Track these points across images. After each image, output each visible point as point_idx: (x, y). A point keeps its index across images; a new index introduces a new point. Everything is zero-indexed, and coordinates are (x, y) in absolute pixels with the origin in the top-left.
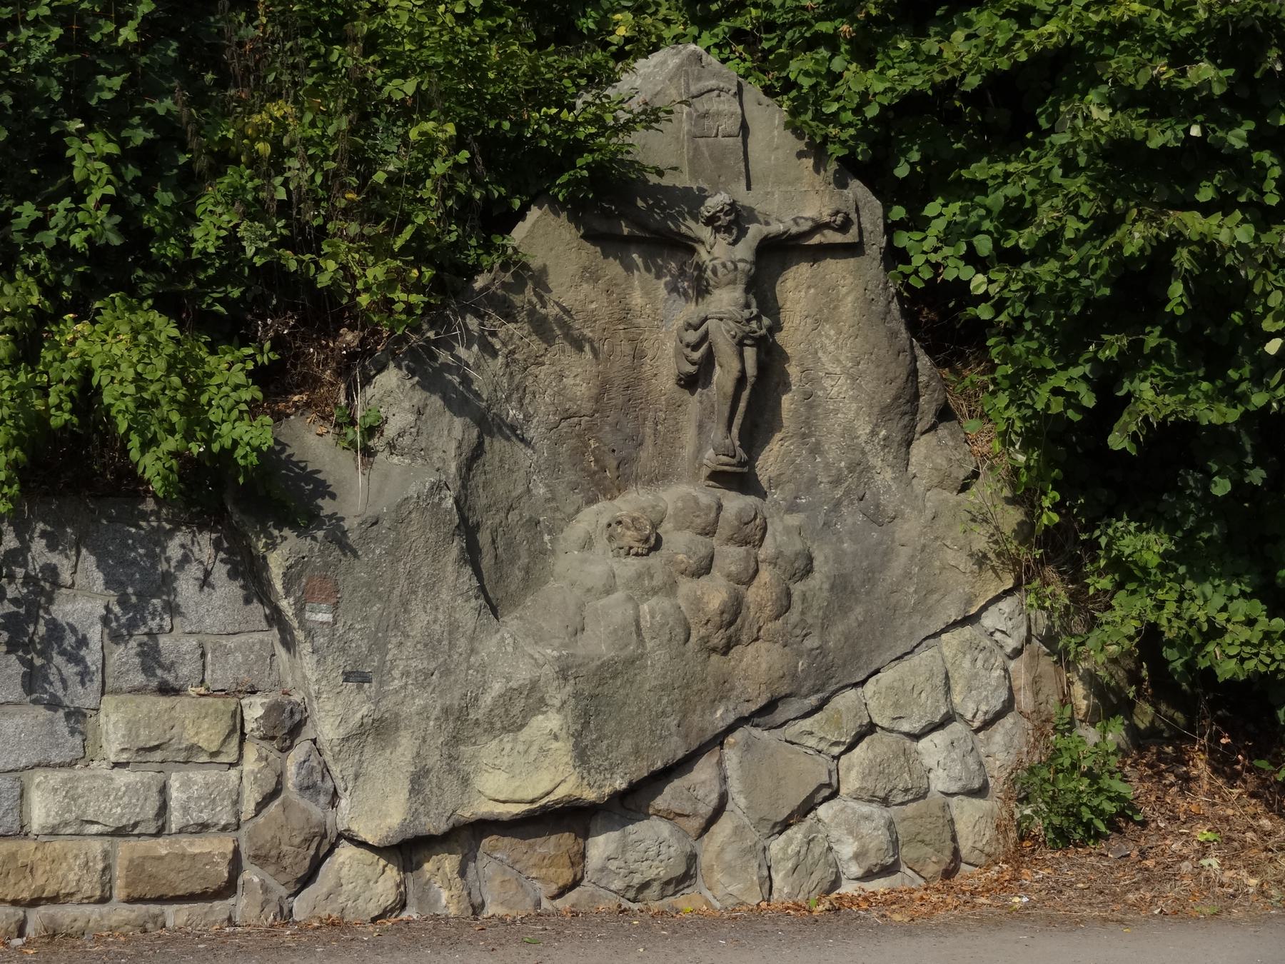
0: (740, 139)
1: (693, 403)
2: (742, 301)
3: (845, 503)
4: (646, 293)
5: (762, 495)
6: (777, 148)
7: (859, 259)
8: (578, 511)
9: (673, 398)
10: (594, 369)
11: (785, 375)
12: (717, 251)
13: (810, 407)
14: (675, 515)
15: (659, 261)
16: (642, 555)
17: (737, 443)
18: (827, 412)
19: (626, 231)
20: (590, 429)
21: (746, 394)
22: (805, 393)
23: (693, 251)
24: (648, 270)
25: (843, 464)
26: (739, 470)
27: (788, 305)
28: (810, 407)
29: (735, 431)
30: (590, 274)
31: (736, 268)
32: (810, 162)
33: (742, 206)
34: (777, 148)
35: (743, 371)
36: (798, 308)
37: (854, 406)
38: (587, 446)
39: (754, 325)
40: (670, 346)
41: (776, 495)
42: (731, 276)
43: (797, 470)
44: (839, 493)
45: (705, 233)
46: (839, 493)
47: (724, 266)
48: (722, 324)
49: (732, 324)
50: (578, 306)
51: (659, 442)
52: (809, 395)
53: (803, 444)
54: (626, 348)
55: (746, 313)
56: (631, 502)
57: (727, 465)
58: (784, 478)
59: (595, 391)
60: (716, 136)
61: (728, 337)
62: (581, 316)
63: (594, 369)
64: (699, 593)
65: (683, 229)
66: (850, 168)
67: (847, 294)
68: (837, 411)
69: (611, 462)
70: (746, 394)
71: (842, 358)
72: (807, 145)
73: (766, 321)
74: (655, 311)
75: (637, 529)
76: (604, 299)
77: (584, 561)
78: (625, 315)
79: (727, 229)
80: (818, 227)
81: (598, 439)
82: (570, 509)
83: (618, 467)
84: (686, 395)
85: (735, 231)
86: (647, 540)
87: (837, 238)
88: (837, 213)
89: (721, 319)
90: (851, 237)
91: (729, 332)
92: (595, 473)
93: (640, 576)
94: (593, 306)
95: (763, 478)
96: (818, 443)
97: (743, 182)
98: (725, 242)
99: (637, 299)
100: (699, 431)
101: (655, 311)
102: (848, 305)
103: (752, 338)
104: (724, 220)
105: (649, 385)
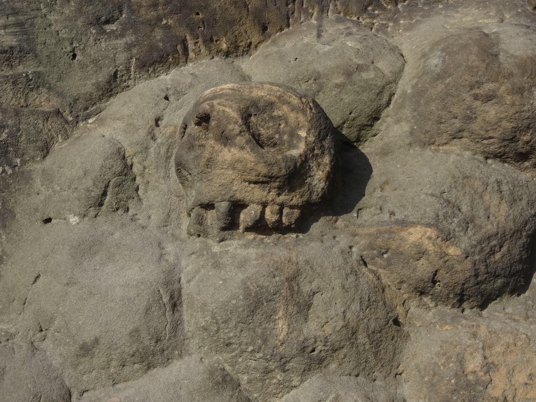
8: (112, 87)
14: (419, 93)
16: (280, 228)
56: (294, 62)
64: (474, 364)
75: (258, 141)
77: (86, 249)
82: (82, 82)
86: (294, 176)
93: (257, 304)
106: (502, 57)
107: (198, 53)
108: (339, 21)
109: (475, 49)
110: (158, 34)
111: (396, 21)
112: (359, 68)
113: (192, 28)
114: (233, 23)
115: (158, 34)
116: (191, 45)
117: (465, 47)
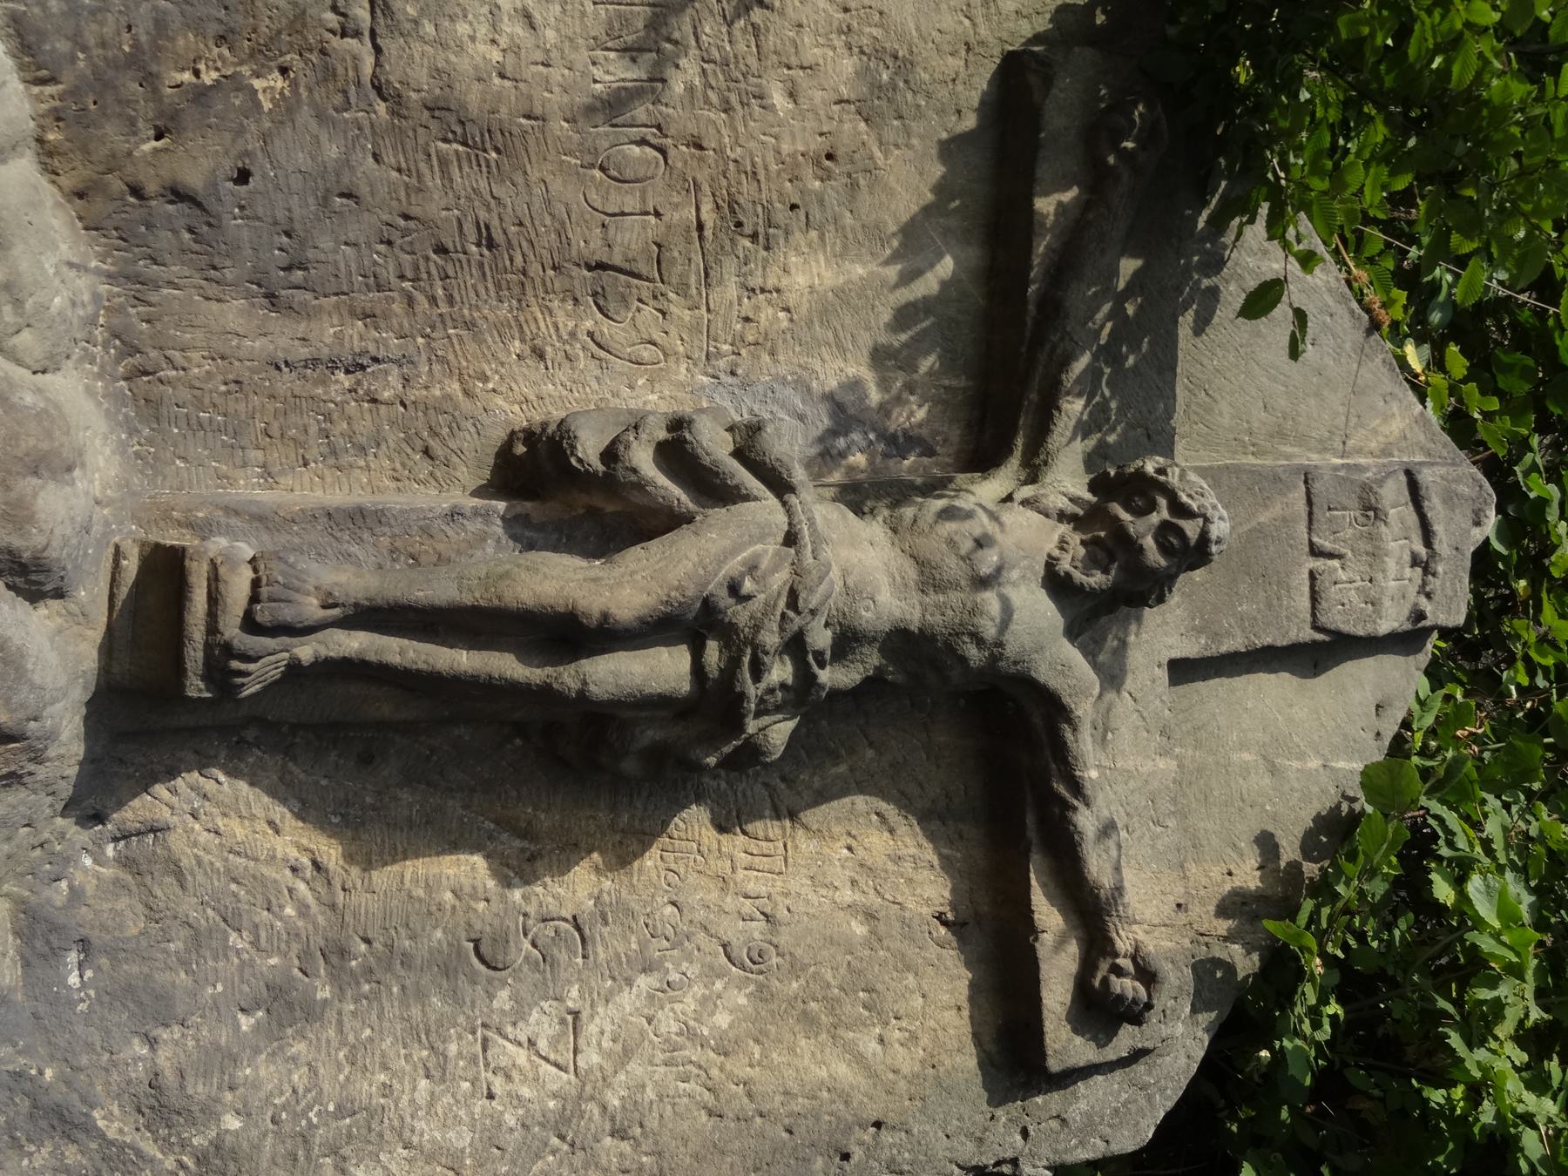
0: (1307, 634)
1: (452, 492)
2: (866, 617)
3: (72, 1155)
4: (833, 305)
5: (91, 803)
6: (1274, 770)
7: (977, 1091)
9: (455, 427)
10: (556, 99)
11: (563, 852)
12: (1021, 524)
13: (448, 967)
15: (928, 363)
17: (306, 651)
18: (428, 1035)
19: (1045, 205)
20: (329, 74)
21: (505, 665)
22: (501, 939)
23: (982, 460)
24: (904, 316)
25: (232, 1123)
26: (195, 655)
27: (806, 845)
28: (448, 967)
29: (354, 643)
30: (886, 86)
31: (982, 583)
32: (1249, 877)
33: (1124, 644)
34: (1274, 770)
35: (606, 636)
36: (798, 883)
37: (462, 1139)
38: (262, 55)
39: (780, 672)
40: (656, 401)
41: (92, 863)
42: (953, 567)
43: (197, 939)
44: (113, 1122)
45: (1068, 480)
46: (113, 1122)
47: (981, 543)
48: (770, 548)
49: (780, 579)
50: (778, 33)
51: (286, 382)
52: (488, 955)
53: (305, 955)
54: (632, 238)
55: (821, 638)
57: (214, 599)
58: (165, 888)
59: (473, 98)
60: (1315, 552)
61: (733, 566)
62: (744, 45)
63: (556, 99)
65: (1074, 408)
66: (1244, 1015)
67: (859, 1059)
68: (438, 1071)
69: (198, 162)
70: (505, 665)
71: (636, 1067)
72: (1294, 867)
73: (779, 732)
74: (766, 344)
76: (801, 140)
78: (746, 225)
79: (1111, 546)
80: (1091, 914)
81: (287, 107)
83: (178, 194)
84: (472, 470)
85: (1096, 580)
87: (1056, 993)
88: (1147, 976)
89: (791, 539)
90: (1064, 1044)
91: (752, 568)
92: (149, 80)
94: (778, 99)
95: (160, 803)
96: (311, 1013)
97: (1190, 648)
98: (1051, 546)
99: (807, 271)
100: (350, 511)
101: (766, 344)
102: (818, 1067)
103: (733, 664)
104: (1143, 529)
105: (500, 328)
106: (34, 481)
107: (38, 99)
108: (96, 297)
109: (45, 446)
110: (63, 46)
111: (100, 376)
112: (18, 303)
113: (74, 93)
114: (86, 150)
115: (63, 46)
116: (49, 90)
117: (49, 435)
